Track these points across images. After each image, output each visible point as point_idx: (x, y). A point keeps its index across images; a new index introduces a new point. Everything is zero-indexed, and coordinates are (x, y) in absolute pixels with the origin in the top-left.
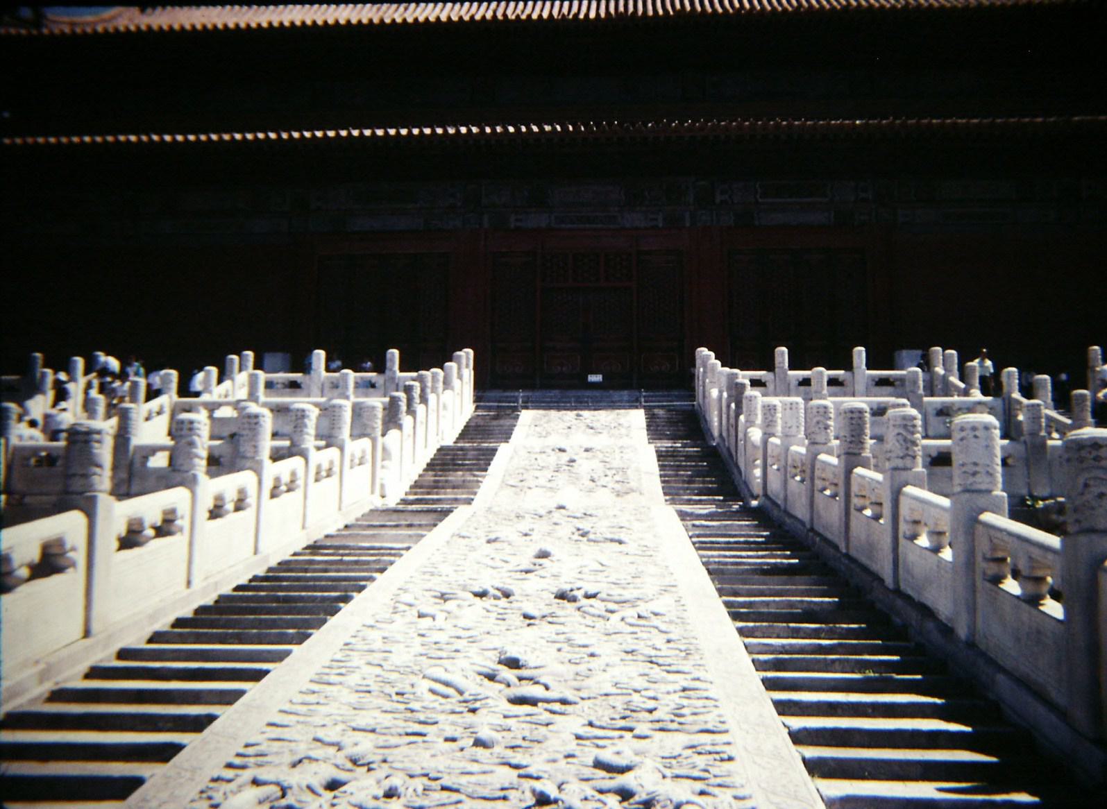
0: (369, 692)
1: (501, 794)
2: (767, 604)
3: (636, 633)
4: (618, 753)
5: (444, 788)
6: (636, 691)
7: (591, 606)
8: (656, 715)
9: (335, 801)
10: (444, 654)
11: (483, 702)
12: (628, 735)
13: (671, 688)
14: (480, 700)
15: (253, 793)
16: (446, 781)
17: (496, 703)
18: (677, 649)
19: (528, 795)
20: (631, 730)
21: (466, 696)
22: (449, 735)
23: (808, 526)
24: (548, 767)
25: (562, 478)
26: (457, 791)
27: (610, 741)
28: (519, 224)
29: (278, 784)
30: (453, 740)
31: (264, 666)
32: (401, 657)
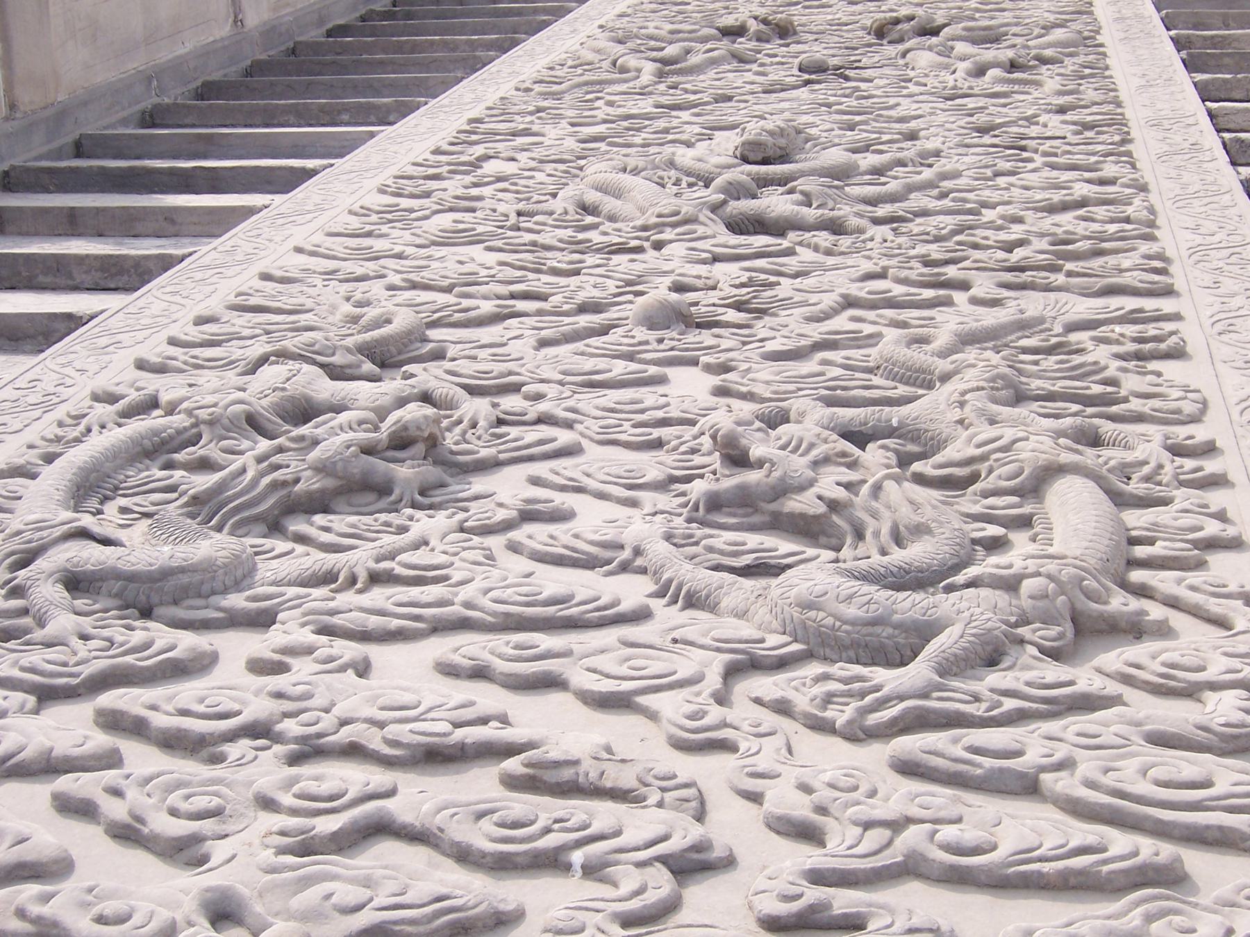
9: (277, 459)
12: (959, 297)
13: (1057, 197)
14: (674, 225)
19: (706, 441)
20: (964, 286)
26: (569, 425)
27: (916, 313)
31: (310, 164)
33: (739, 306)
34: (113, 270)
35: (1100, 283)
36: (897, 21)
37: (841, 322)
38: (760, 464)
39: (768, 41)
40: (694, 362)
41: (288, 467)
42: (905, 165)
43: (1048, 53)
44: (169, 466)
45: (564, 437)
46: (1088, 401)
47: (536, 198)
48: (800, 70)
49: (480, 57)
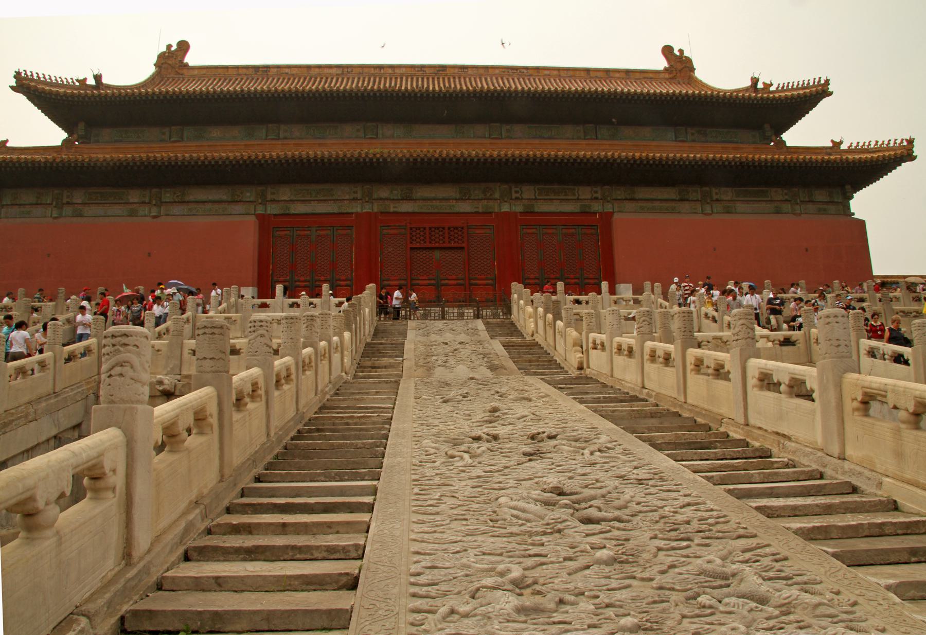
0: (466, 520)
2: (663, 437)
4: (709, 562)
11: (564, 524)
14: (560, 523)
22: (564, 554)
26: (621, 607)
28: (395, 210)
30: (570, 559)
32: (464, 488)
36: (539, 434)
43: (609, 445)
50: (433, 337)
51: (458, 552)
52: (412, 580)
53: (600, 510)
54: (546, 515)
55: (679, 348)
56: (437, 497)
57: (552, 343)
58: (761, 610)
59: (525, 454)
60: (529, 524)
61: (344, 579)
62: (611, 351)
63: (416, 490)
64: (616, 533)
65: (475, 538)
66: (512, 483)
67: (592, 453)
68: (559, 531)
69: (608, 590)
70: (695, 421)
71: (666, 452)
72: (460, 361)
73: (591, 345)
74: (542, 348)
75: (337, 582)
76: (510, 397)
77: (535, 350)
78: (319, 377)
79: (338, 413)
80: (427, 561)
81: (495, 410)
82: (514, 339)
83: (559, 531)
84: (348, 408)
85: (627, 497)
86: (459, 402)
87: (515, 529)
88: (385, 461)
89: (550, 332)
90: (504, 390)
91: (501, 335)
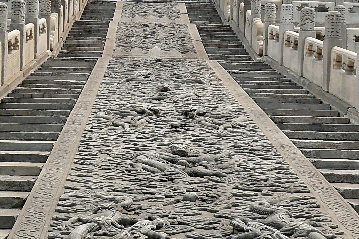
0: (110, 169)
1: (212, 226)
3: (235, 136)
4: (261, 204)
5: (180, 223)
6: (251, 169)
7: (206, 121)
8: (269, 182)
9: (133, 231)
10: (140, 148)
11: (176, 175)
13: (269, 167)
14: (174, 174)
15: (82, 229)
16: (179, 219)
17: (184, 176)
18: (261, 146)
21: (166, 172)
23: (300, 75)
24: (228, 211)
25: (149, 43)
29: (96, 222)
30: (170, 196)
32: (117, 148)
33: (207, 196)
34: (12, 185)
35: (293, 190)
36: (191, 111)
37: (234, 200)
38: (247, 231)
39: (152, 116)
40: (207, 210)
41: (136, 233)
42: (223, 158)
44: (95, 235)
45: (190, 228)
46: (306, 217)
47: (127, 166)
48: (172, 127)
49: (61, 118)
50: (138, 19)
51: (96, 189)
52: (60, 203)
53: (206, 168)
54: (165, 169)
55: (326, 45)
56: (95, 154)
57: (242, 30)
58: (269, 230)
59: (173, 126)
60: (152, 175)
61: (16, 202)
62: (283, 43)
63: (82, 148)
64: (211, 183)
65: (111, 181)
66: (154, 146)
67: (225, 129)
68: (172, 180)
69: (185, 215)
70: (331, 108)
71: (287, 131)
72: (157, 43)
73: (269, 36)
74: (234, 34)
75: (11, 204)
76: (185, 79)
77: (228, 34)
78: (24, 55)
79: (37, 87)
80: (73, 193)
81: (165, 90)
82: (213, 24)
83: (172, 180)
84: (46, 82)
85: (233, 161)
86: (140, 82)
87: (141, 177)
88: (65, 127)
89: (241, 20)
90: (180, 73)
91: (201, 19)
